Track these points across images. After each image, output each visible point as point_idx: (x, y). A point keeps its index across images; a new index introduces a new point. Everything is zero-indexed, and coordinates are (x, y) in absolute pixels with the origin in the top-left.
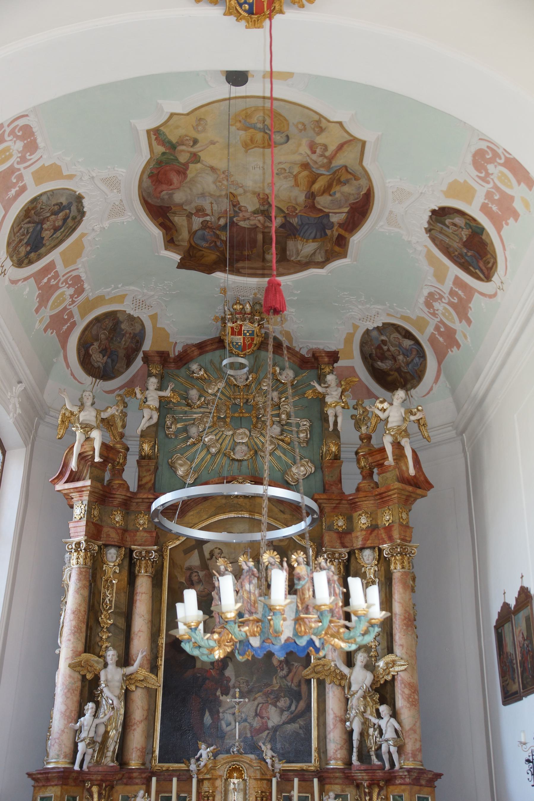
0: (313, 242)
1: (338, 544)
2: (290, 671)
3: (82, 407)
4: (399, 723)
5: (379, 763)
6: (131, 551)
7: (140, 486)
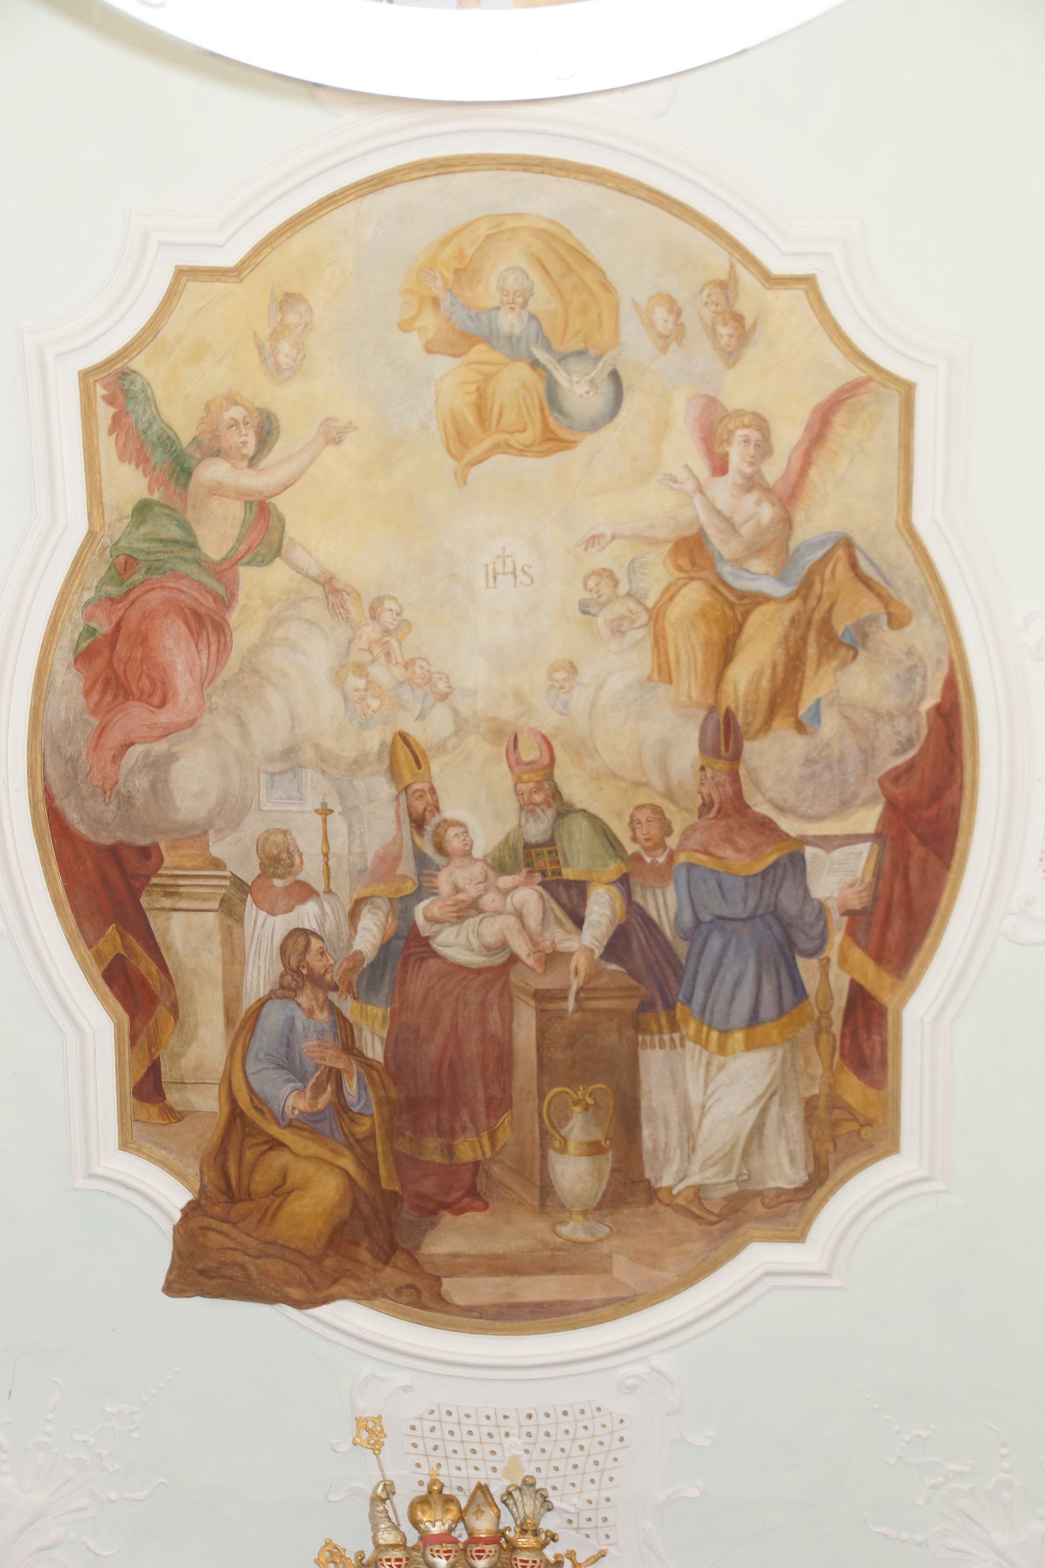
0: (750, 1046)
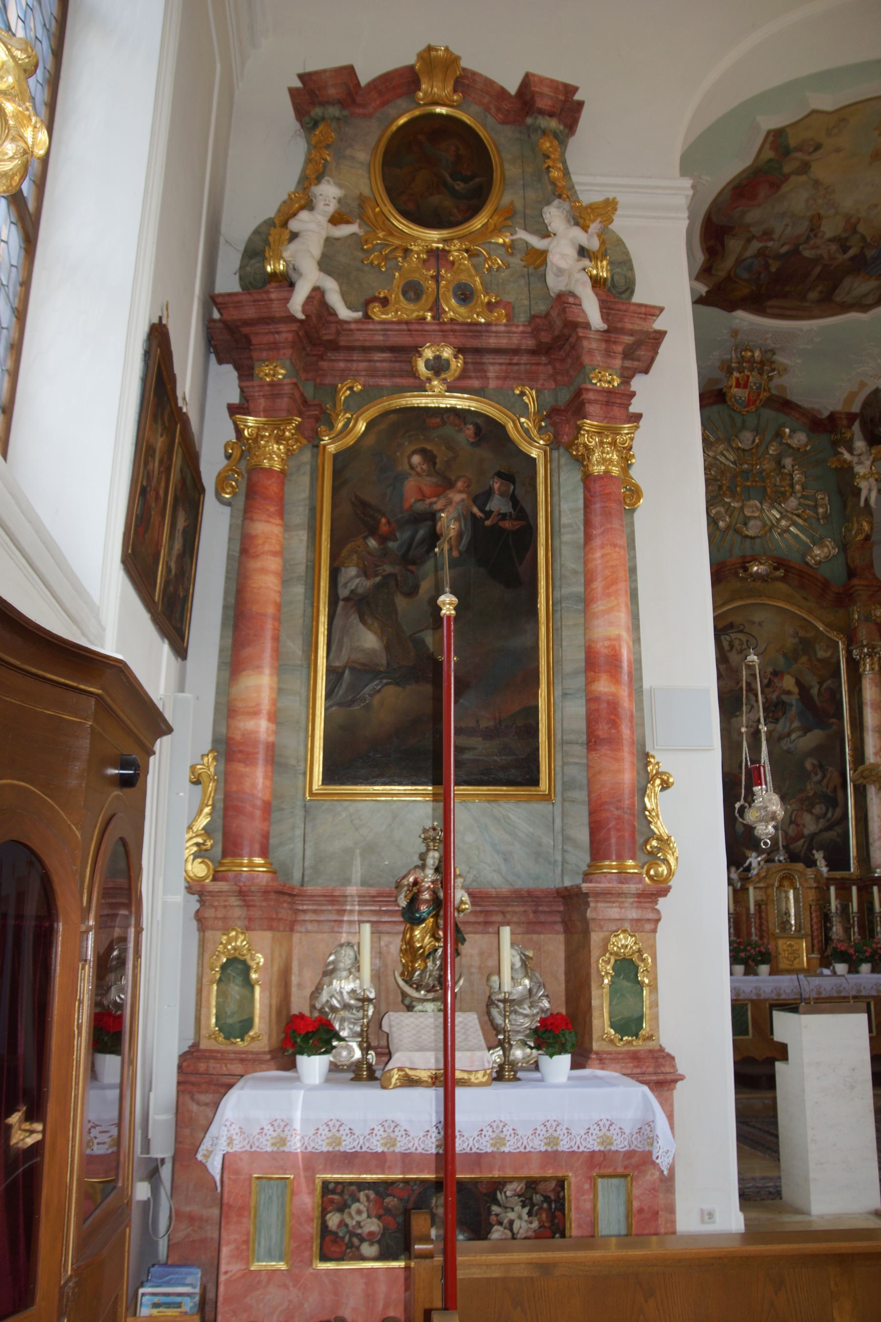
2: (824, 777)
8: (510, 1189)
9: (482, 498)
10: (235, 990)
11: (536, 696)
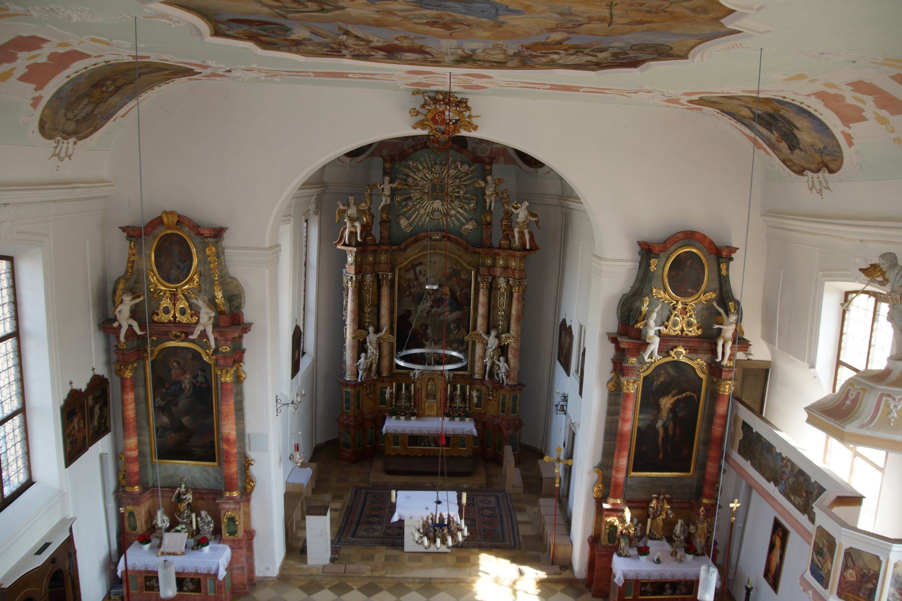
1: (487, 274)
2: (458, 332)
3: (348, 205)
4: (508, 365)
5: (498, 379)
6: (378, 275)
7: (381, 238)
8: (187, 579)
9: (195, 377)
10: (132, 519)
11: (214, 437)
